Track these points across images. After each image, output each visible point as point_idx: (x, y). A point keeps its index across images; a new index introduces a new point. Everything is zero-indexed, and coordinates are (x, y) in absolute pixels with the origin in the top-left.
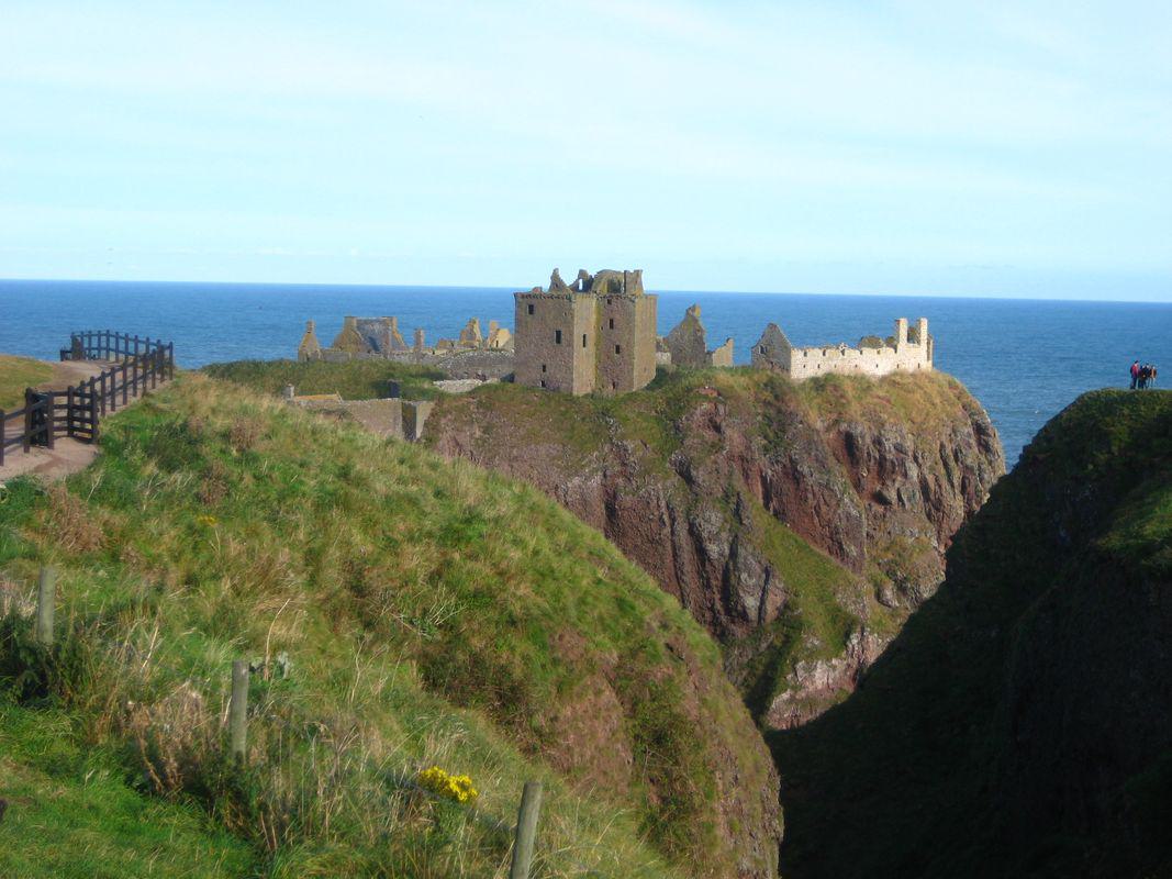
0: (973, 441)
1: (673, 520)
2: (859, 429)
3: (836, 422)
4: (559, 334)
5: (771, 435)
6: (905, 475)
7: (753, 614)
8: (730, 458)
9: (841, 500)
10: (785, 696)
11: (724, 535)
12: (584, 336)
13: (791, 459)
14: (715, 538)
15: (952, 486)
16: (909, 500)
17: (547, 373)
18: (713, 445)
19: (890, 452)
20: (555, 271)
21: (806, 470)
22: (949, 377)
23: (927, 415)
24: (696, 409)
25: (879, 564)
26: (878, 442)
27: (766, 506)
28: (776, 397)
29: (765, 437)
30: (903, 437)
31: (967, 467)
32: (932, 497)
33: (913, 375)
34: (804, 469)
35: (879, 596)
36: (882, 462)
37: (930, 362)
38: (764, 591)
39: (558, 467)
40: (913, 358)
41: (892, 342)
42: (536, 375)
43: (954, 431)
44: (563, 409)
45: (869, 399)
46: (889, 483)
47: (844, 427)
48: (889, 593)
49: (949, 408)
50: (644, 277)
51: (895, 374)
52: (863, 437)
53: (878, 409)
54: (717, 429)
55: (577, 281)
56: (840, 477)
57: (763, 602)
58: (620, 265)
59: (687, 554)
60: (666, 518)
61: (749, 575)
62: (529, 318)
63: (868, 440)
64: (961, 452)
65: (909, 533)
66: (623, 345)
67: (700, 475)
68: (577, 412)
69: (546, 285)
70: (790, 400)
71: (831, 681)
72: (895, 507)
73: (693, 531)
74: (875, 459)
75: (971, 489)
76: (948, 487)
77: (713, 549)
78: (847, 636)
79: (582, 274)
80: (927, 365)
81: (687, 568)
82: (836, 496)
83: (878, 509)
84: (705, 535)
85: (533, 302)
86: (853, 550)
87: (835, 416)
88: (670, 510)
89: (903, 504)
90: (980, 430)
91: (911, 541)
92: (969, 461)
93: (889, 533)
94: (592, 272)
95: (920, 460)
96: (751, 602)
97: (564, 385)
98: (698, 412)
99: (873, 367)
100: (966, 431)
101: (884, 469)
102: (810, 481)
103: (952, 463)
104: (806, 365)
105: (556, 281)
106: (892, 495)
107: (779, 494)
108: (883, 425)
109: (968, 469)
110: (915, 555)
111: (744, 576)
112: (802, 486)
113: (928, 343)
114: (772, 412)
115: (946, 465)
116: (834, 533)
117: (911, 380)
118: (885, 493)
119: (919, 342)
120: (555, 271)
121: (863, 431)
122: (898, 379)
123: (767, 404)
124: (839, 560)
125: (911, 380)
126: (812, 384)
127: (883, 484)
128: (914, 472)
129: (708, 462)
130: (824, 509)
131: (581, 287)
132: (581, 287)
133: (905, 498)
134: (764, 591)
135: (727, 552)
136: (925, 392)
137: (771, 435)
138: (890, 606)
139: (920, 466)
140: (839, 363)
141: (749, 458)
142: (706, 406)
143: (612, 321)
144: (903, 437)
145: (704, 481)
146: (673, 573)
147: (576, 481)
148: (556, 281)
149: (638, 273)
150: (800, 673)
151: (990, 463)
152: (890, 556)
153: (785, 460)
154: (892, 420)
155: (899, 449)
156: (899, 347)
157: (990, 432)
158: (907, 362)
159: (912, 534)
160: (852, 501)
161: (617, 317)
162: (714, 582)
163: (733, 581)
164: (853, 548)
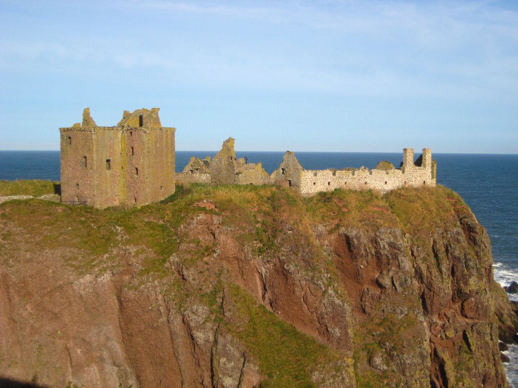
2: (354, 233)
3: (338, 226)
5: (265, 239)
9: (325, 292)
13: (280, 261)
14: (201, 327)
15: (441, 272)
16: (401, 285)
18: (207, 249)
21: (292, 268)
22: (449, 191)
23: (423, 218)
24: (193, 219)
25: (373, 336)
26: (375, 241)
28: (274, 208)
29: (261, 241)
30: (395, 237)
31: (455, 257)
32: (425, 280)
33: (416, 189)
35: (370, 361)
36: (378, 256)
37: (435, 180)
39: (72, 266)
40: (424, 177)
41: (400, 165)
43: (446, 231)
44: (83, 219)
45: (370, 208)
46: (385, 272)
47: (342, 230)
49: (443, 214)
50: (160, 114)
51: (403, 188)
52: (358, 239)
53: (376, 215)
58: (149, 105)
59: (181, 341)
61: (227, 359)
63: (364, 240)
65: (399, 311)
66: (140, 169)
67: (190, 274)
68: (94, 222)
70: (284, 211)
74: (372, 254)
75: (458, 274)
76: (437, 274)
77: (200, 336)
80: (431, 182)
81: (180, 350)
82: (321, 288)
83: (377, 291)
84: (192, 324)
85: (70, 134)
87: (336, 222)
89: (396, 289)
90: (469, 230)
91: (400, 317)
92: (457, 253)
93: (383, 311)
97: (89, 200)
98: (195, 221)
99: (383, 184)
100: (455, 230)
101: (381, 262)
103: (442, 255)
104: (313, 183)
106: (386, 282)
107: (272, 287)
108: (378, 228)
110: (402, 329)
111: (223, 360)
112: (289, 281)
113: (433, 166)
114: (269, 220)
115: (436, 256)
116: (321, 318)
117: (414, 193)
119: (425, 166)
121: (359, 233)
122: (403, 192)
123: (266, 214)
124: (325, 339)
125: (414, 193)
126: (319, 198)
127: (381, 273)
128: (407, 265)
129: (200, 263)
130: (311, 299)
133: (397, 284)
136: (424, 202)
137: (265, 239)
140: (349, 181)
141: (243, 258)
144: (395, 237)
145: (193, 279)
146: (172, 353)
147: (88, 278)
149: (155, 111)
151: (477, 253)
152: (382, 330)
153: (276, 260)
154: (387, 225)
156: (407, 170)
157: (477, 230)
158: (414, 180)
159: (402, 312)
160: (336, 292)
161: (136, 146)
162: (202, 363)
164: (337, 330)
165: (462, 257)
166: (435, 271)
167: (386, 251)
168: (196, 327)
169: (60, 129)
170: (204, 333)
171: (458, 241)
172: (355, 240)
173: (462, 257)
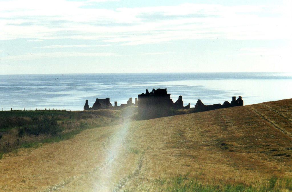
20: (147, 89)
55: (152, 92)
69: (145, 93)
79: (153, 90)
94: (156, 89)
105: (147, 91)
120: (147, 89)
149: (166, 89)
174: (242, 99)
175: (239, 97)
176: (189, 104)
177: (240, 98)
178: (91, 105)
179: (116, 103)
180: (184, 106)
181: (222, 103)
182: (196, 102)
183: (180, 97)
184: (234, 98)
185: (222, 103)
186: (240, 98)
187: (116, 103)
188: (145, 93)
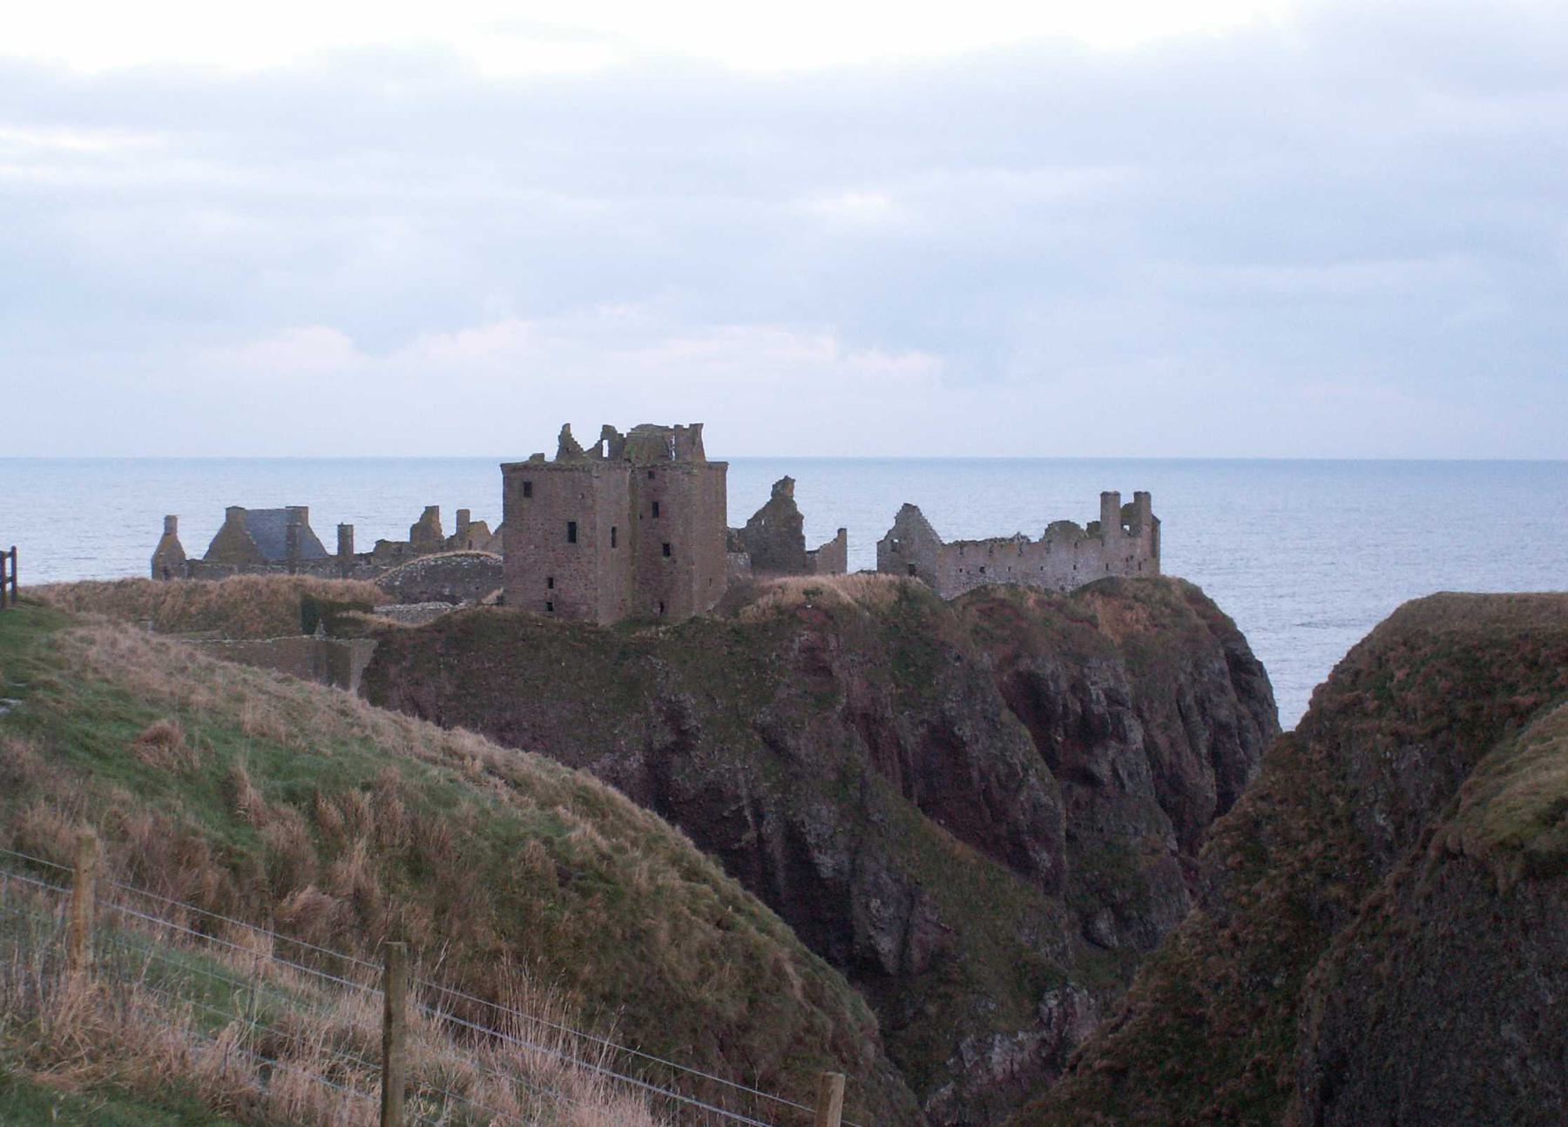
0: (1227, 683)
1: (759, 816)
4: (572, 527)
6: (1123, 739)
7: (891, 964)
8: (848, 716)
10: (946, 1092)
11: (841, 840)
12: (614, 529)
15: (1198, 755)
17: (555, 591)
19: (1098, 702)
20: (566, 427)
24: (792, 641)
26: (1078, 687)
27: (907, 794)
34: (965, 731)
38: (907, 928)
42: (540, 592)
47: (1025, 664)
48: (1103, 925)
50: (706, 436)
52: (1056, 682)
54: (826, 671)
55: (599, 446)
56: (1021, 744)
57: (904, 944)
58: (667, 418)
60: (747, 813)
61: (883, 903)
62: (526, 503)
63: (1064, 685)
64: (1210, 700)
65: (1132, 830)
66: (674, 542)
67: (801, 745)
69: (551, 455)
71: (1016, 1067)
72: (1109, 789)
73: (794, 836)
76: (1192, 758)
77: (826, 863)
78: (1039, 997)
79: (608, 431)
83: (1080, 791)
84: (811, 840)
85: (528, 477)
86: (1044, 859)
88: (757, 805)
89: (1123, 786)
94: (623, 429)
95: (1147, 715)
96: (886, 944)
98: (796, 646)
102: (975, 750)
105: (566, 439)
106: (1103, 770)
109: (1222, 728)
111: (875, 903)
118: (1095, 768)
120: (566, 427)
128: (1137, 735)
131: (605, 454)
132: (605, 454)
133: (1123, 774)
134: (907, 928)
135: (847, 866)
138: (1106, 948)
139: (1145, 722)
142: (807, 636)
143: (656, 506)
144: (1117, 678)
145: (807, 755)
148: (566, 439)
149: (696, 429)
150: (970, 1056)
151: (1256, 715)
155: (1113, 698)
159: (1137, 832)
161: (665, 499)
163: (857, 910)
164: (1045, 855)
165: (1234, 722)
166: (1186, 750)
167: (1098, 709)
168: (817, 845)
169: (502, 466)
170: (832, 857)
171: (1222, 689)
172: (1051, 684)
173: (1234, 722)
174: (1156, 511)
175: (1137, 494)
176: (842, 531)
177: (1142, 498)
178: (195, 546)
179: (345, 533)
180: (811, 544)
181: (1035, 534)
182: (885, 523)
183: (783, 490)
184: (1108, 498)
185: (1035, 534)
186: (1142, 498)
187: (345, 533)
188: (551, 455)
